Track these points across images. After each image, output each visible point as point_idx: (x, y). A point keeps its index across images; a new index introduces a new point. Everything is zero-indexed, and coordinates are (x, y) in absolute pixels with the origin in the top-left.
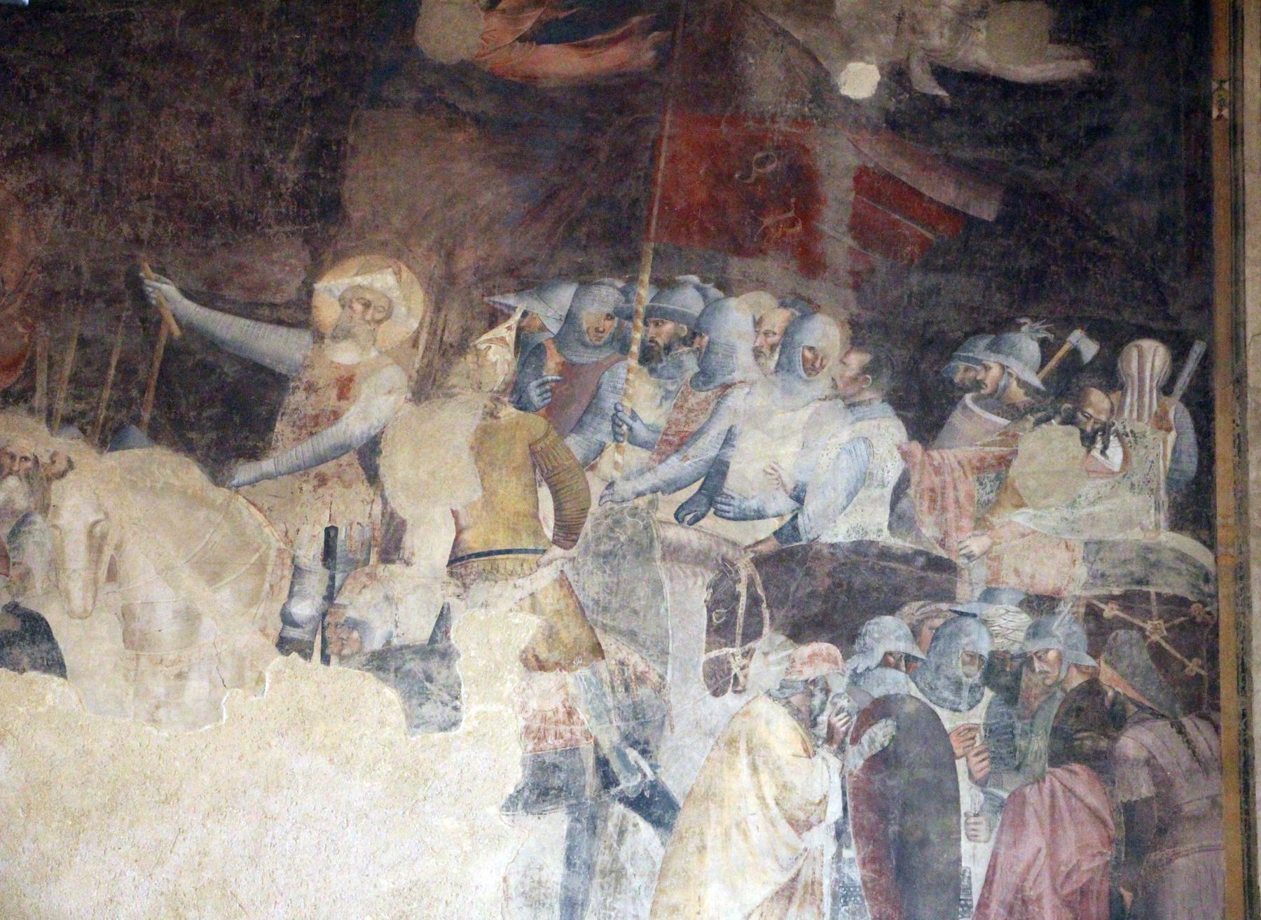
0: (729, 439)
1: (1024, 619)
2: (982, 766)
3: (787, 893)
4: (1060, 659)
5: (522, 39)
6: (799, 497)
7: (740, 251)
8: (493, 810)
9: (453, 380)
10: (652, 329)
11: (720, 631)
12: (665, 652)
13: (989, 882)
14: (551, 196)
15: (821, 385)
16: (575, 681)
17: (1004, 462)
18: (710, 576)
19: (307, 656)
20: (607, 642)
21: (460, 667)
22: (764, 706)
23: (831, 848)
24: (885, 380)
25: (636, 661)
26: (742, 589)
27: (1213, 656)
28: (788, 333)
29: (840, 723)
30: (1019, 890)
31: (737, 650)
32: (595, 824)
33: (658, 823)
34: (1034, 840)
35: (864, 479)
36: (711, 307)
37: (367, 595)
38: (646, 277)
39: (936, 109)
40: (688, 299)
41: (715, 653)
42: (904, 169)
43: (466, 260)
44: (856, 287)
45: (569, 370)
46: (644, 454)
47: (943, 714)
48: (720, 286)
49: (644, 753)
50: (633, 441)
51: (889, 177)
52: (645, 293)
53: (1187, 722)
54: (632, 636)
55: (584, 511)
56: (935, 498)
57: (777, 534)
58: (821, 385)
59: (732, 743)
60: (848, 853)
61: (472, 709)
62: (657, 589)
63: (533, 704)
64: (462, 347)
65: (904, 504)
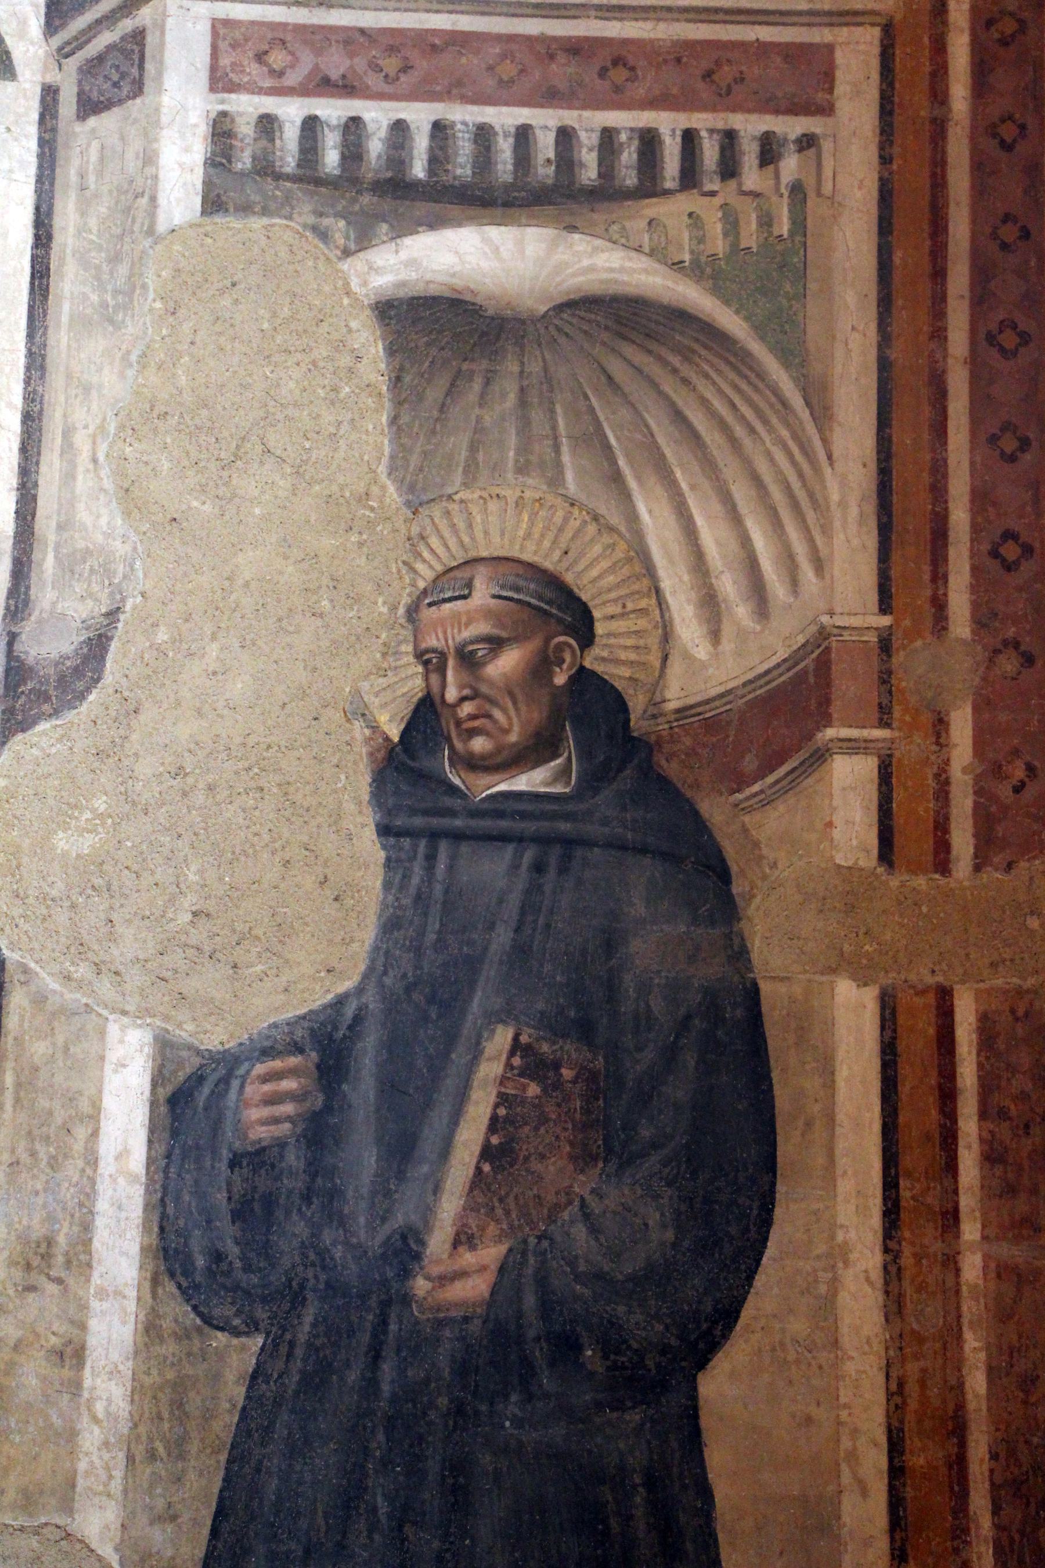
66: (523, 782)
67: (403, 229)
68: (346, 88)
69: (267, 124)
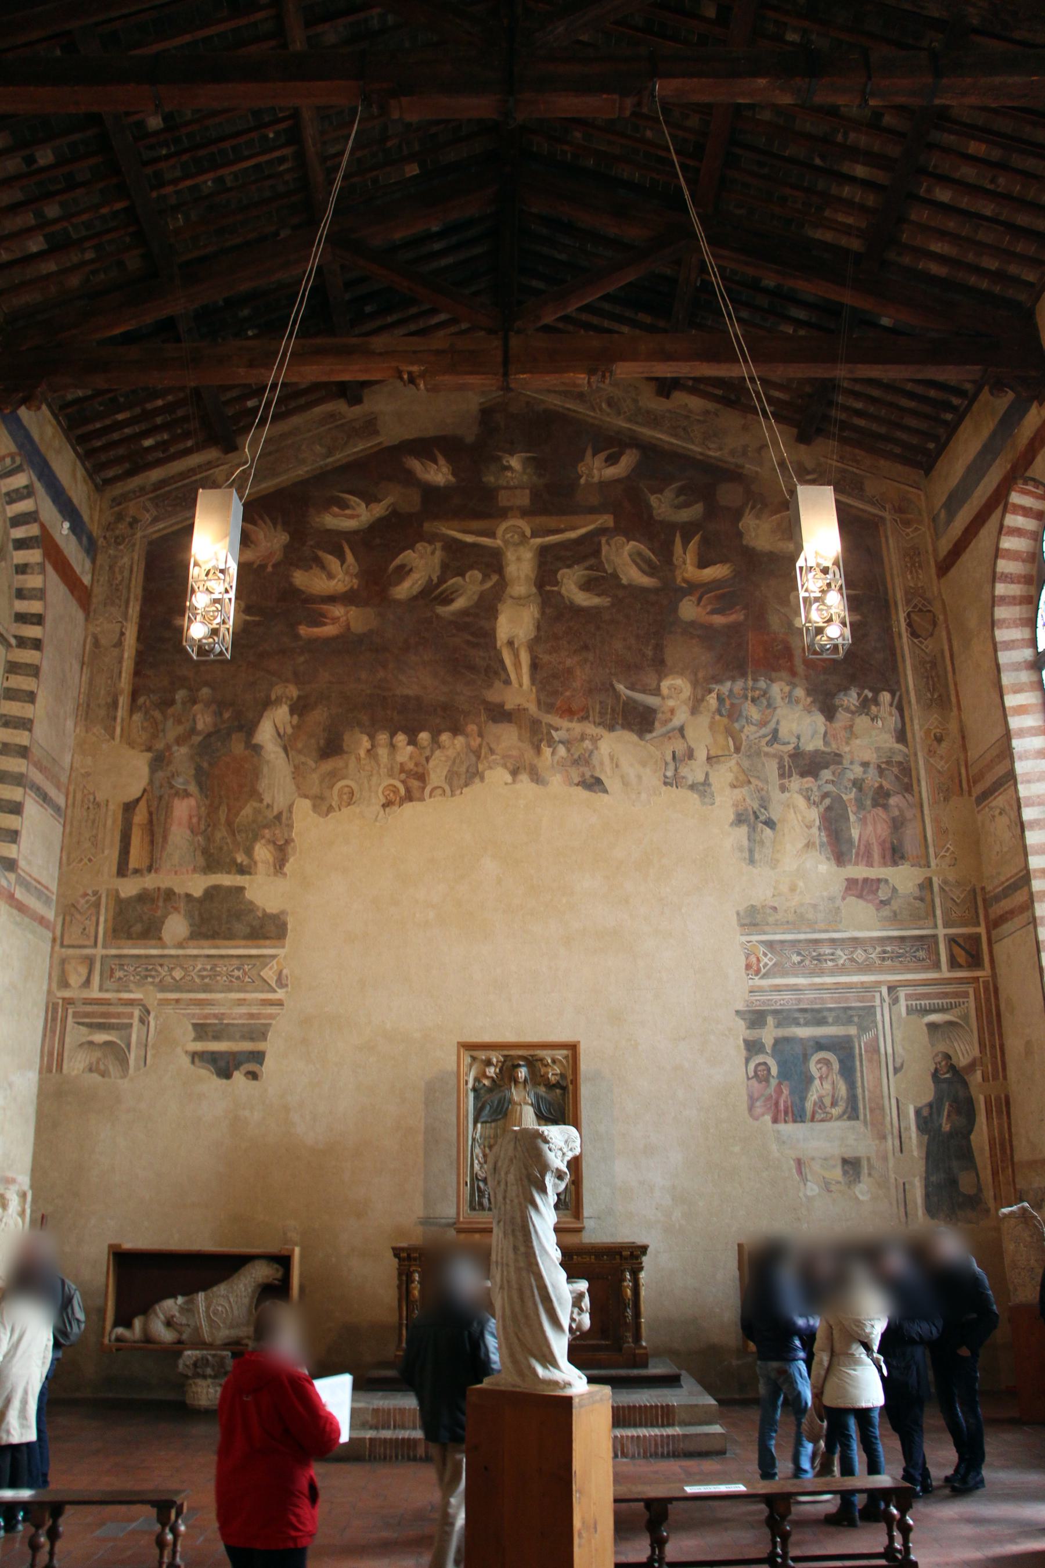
0: (778, 723)
1: (861, 769)
2: (854, 809)
4: (872, 779)
5: (708, 613)
6: (798, 737)
7: (774, 670)
8: (727, 827)
9: (701, 709)
10: (753, 693)
11: (782, 776)
12: (767, 782)
15: (801, 707)
16: (744, 790)
17: (851, 726)
18: (777, 761)
19: (672, 786)
20: (752, 780)
21: (713, 788)
22: (796, 795)
23: (817, 833)
25: (760, 784)
26: (786, 764)
28: (790, 692)
29: (816, 799)
30: (868, 841)
31: (787, 780)
34: (870, 828)
35: (815, 733)
36: (768, 686)
37: (686, 770)
38: (750, 678)
40: (762, 684)
41: (781, 782)
43: (701, 675)
44: (807, 679)
45: (732, 705)
47: (843, 796)
48: (770, 680)
49: (765, 809)
50: (752, 724)
52: (750, 683)
53: (906, 795)
54: (758, 778)
55: (741, 744)
56: (834, 737)
57: (794, 748)
58: (801, 707)
59: (788, 806)
60: (823, 834)
61: (718, 799)
62: (764, 765)
63: (734, 797)
64: (702, 700)
65: (827, 739)
66: (947, 1076)
67: (927, 1015)
68: (919, 999)
69: (912, 1005)
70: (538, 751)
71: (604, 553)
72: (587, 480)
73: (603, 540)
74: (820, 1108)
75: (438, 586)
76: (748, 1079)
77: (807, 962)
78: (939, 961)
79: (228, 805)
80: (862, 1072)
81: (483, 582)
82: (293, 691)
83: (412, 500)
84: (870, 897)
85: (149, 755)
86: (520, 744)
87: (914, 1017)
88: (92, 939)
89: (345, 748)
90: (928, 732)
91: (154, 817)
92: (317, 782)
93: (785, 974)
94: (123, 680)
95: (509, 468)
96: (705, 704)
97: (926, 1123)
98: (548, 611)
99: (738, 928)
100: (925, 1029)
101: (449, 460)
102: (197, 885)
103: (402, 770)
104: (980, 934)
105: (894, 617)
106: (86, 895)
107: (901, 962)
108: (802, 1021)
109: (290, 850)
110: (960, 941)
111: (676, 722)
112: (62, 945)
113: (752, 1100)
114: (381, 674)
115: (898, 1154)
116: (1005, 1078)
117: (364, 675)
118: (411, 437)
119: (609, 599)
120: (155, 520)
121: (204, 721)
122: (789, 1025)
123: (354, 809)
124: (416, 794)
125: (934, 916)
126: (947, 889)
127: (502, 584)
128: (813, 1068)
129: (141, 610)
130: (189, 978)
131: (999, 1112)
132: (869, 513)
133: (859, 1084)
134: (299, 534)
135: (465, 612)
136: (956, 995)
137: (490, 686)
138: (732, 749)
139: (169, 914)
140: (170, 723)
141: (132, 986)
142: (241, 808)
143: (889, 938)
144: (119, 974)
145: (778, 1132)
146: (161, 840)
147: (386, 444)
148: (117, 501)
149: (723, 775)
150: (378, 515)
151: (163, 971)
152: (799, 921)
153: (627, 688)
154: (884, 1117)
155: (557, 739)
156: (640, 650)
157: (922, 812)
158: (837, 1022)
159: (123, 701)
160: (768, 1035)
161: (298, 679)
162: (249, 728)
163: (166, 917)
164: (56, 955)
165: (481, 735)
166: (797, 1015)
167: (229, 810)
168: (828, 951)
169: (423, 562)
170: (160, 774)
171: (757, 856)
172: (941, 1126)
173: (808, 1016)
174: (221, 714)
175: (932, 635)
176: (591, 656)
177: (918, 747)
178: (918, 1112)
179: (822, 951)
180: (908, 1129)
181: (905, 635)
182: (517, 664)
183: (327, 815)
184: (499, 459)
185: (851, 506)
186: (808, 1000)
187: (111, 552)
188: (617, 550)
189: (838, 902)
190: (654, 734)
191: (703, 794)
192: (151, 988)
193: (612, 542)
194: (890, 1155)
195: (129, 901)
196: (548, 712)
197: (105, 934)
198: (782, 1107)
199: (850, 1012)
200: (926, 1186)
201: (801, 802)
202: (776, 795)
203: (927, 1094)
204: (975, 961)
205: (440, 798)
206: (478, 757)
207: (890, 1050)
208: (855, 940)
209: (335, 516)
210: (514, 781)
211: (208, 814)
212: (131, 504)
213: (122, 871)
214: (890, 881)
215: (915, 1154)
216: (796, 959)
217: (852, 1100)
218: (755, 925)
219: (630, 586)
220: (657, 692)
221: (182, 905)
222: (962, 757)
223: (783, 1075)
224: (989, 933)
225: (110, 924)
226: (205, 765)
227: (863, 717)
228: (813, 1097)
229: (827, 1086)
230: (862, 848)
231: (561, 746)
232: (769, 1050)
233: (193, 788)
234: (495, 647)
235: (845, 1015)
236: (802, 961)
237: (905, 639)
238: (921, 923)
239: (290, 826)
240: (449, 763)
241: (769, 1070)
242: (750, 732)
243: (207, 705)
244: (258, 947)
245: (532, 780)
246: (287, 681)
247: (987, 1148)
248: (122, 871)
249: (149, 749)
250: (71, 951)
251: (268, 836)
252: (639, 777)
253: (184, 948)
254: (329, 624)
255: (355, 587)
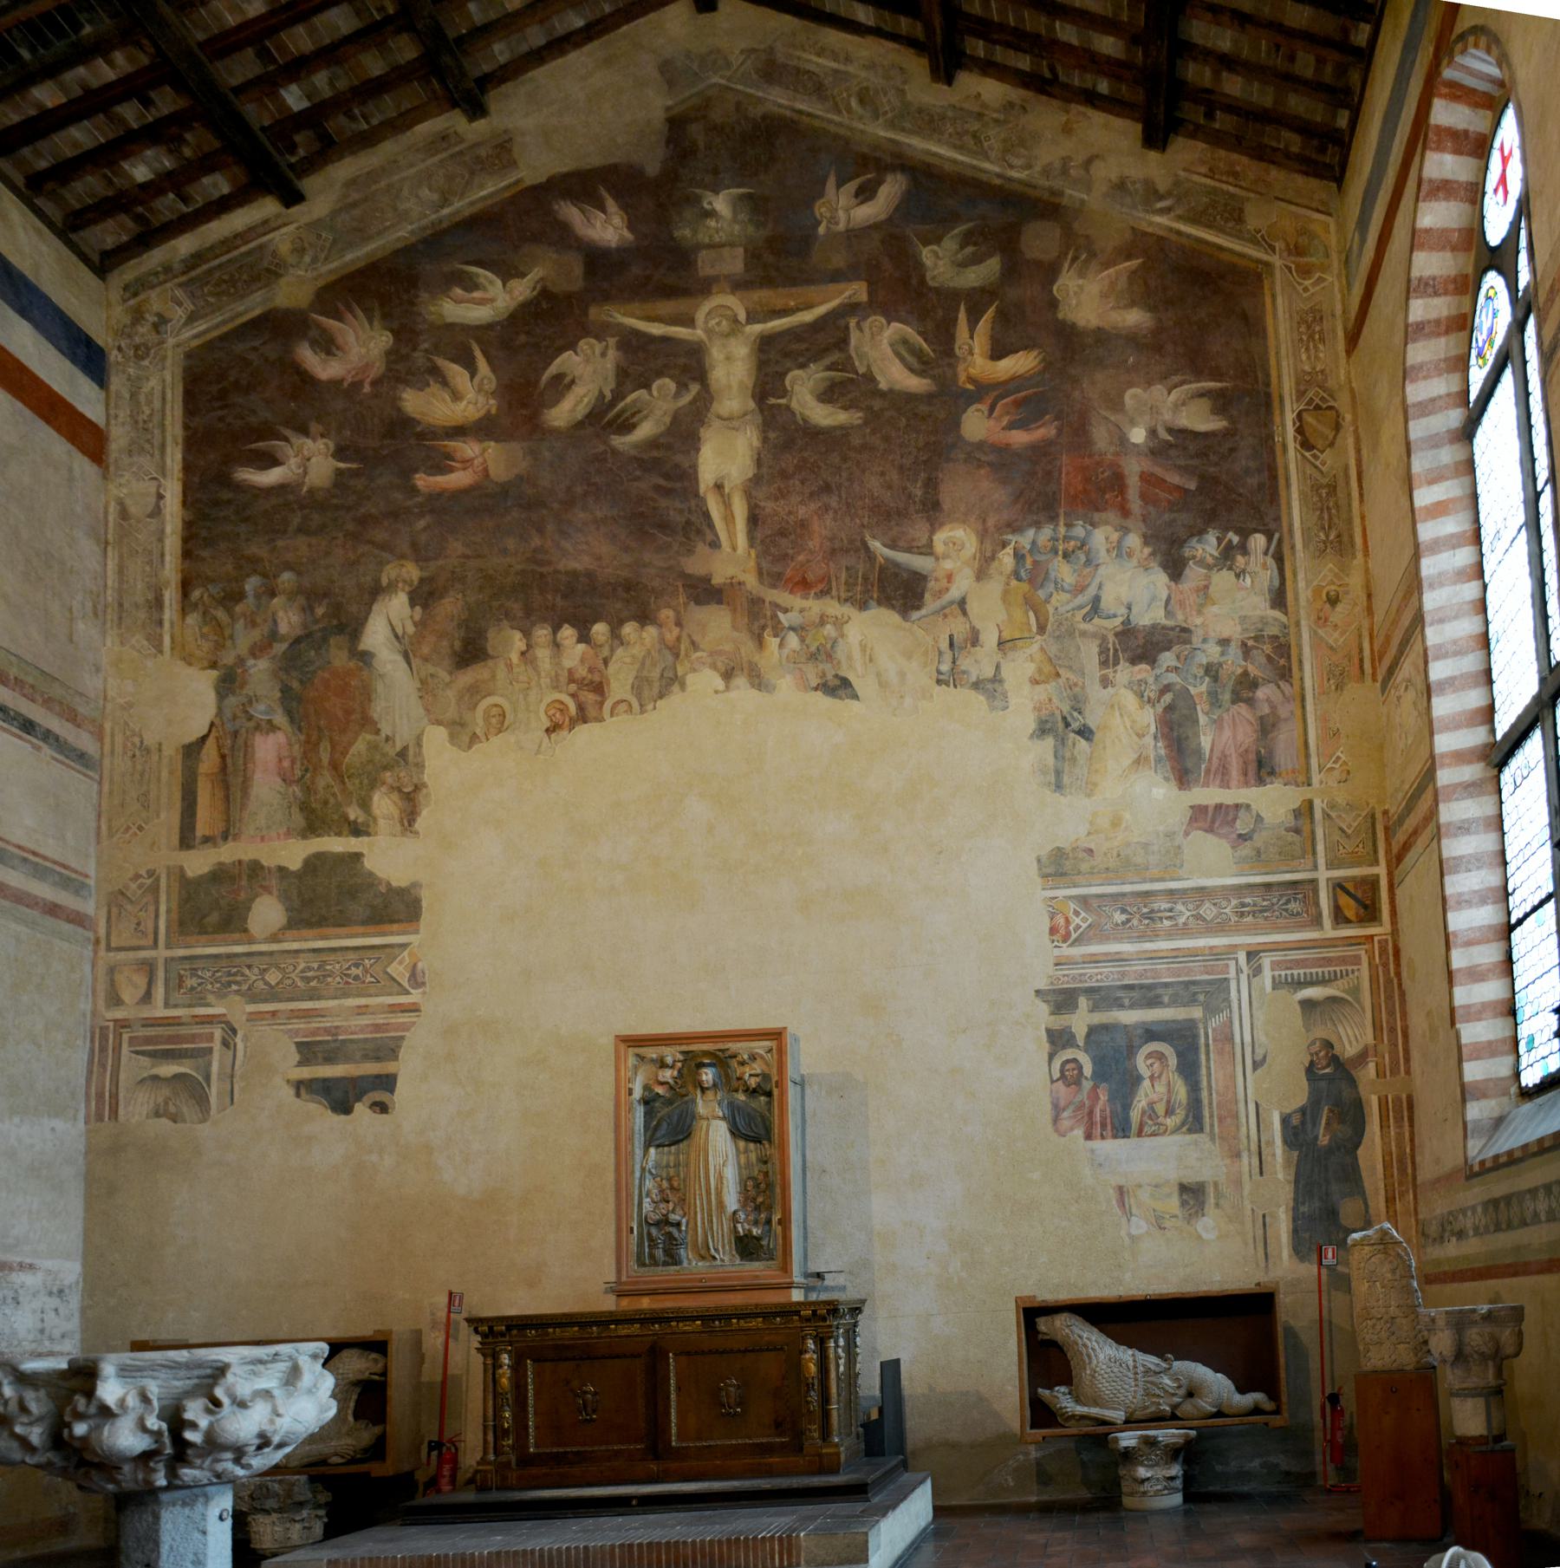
0: (1100, 587)
1: (1218, 649)
2: (1207, 707)
3: (1138, 761)
7: (1097, 510)
11: (1104, 664)
13: (1212, 750)
14: (1021, 493)
15: (1134, 562)
16: (1051, 687)
17: (1206, 587)
18: (1098, 642)
20: (1061, 671)
21: (1007, 686)
22: (1123, 691)
23: (1153, 743)
24: (1158, 558)
27: (1289, 657)
28: (1119, 542)
29: (1152, 695)
32: (1063, 741)
33: (1087, 739)
34: (1227, 733)
35: (1153, 599)
36: (1088, 533)
39: (1171, 446)
40: (1079, 531)
42: (1159, 471)
43: (991, 522)
45: (1035, 563)
46: (1068, 596)
51: (1152, 474)
52: (1062, 530)
54: (1070, 668)
58: (1134, 562)
60: (1160, 744)
61: (1013, 701)
62: (1079, 649)
64: (993, 558)
70: (760, 642)
71: (853, 342)
72: (828, 228)
73: (853, 323)
74: (1150, 1118)
75: (612, 404)
76: (1053, 1082)
77: (1135, 922)
78: (1320, 915)
79: (331, 740)
80: (1208, 1068)
81: (677, 395)
82: (412, 572)
83: (564, 272)
84: (1225, 830)
85: (214, 674)
86: (736, 634)
87: (1282, 992)
88: (151, 937)
89: (490, 651)
90: (1317, 591)
91: (229, 761)
92: (453, 701)
93: (1104, 938)
94: (167, 566)
95: (711, 214)
96: (995, 564)
97: (1296, 1135)
98: (772, 435)
99: (1039, 880)
100: (1298, 1008)
101: (624, 207)
102: (293, 853)
103: (571, 680)
104: (1378, 876)
105: (1277, 419)
106: (137, 876)
107: (1266, 918)
108: (1126, 1002)
109: (421, 797)
110: (1350, 886)
111: (955, 593)
112: (109, 948)
113: (1057, 1110)
114: (536, 541)
115: (1256, 1177)
116: (1408, 1072)
117: (511, 543)
118: (565, 170)
119: (860, 414)
120: (192, 318)
121: (289, 620)
122: (1109, 1008)
123: (508, 738)
124: (591, 712)
125: (1314, 853)
126: (1333, 814)
127: (706, 397)
128: (1142, 1064)
129: (184, 459)
130: (289, 982)
131: (1399, 1119)
132: (1250, 258)
133: (1204, 1084)
134: (405, 334)
135: (653, 443)
136: (1343, 960)
137: (690, 552)
138: (1034, 629)
139: (257, 896)
140: (240, 625)
141: (211, 998)
142: (351, 744)
143: (1250, 886)
144: (191, 982)
145: (1092, 1151)
146: (239, 794)
147: (528, 182)
148: (134, 289)
149: (1019, 669)
150: (521, 298)
151: (252, 975)
152: (1124, 866)
153: (885, 545)
154: (1238, 1127)
155: (786, 625)
156: (905, 489)
157: (1304, 707)
158: (1175, 1002)
159: (171, 596)
160: (1080, 1021)
161: (419, 554)
162: (350, 627)
163: (252, 900)
164: (100, 962)
165: (679, 624)
166: (1120, 994)
167: (333, 747)
168: (1165, 906)
169: (590, 369)
170: (232, 701)
171: (1066, 780)
172: (1316, 1138)
173: (1135, 994)
174: (312, 609)
175: (1332, 444)
176: (833, 502)
177: (1302, 612)
178: (1285, 1120)
179: (1156, 906)
180: (1271, 1143)
181: (1292, 445)
182: (729, 518)
183: (470, 747)
184: (698, 200)
185: (1220, 248)
186: (1134, 973)
187: (131, 371)
188: (873, 337)
189: (1179, 839)
190: (923, 612)
191: (991, 696)
192: (237, 998)
193: (866, 325)
194: (1246, 1177)
195: (199, 881)
196: (774, 586)
197: (168, 928)
198: (1098, 1118)
199: (1194, 989)
200: (1294, 1220)
201: (1129, 700)
202: (1096, 693)
203: (1300, 1096)
204: (1369, 912)
205: (625, 716)
206: (677, 656)
207: (1248, 1038)
208: (1202, 889)
209: (458, 301)
210: (727, 688)
211: (305, 755)
212: (153, 294)
213: (187, 839)
214: (1253, 807)
215: (1280, 1176)
216: (1119, 917)
217: (1195, 1106)
218: (1063, 874)
219: (891, 391)
220: (928, 550)
221: (274, 882)
222: (1366, 624)
223: (1100, 1075)
224: (1390, 874)
225: (175, 916)
226: (295, 685)
227: (1225, 572)
228: (1140, 1103)
229: (1161, 1088)
230: (1215, 761)
231: (792, 634)
232: (1081, 1044)
233: (280, 718)
234: (697, 495)
235: (1187, 992)
236: (1128, 921)
237: (1291, 453)
238: (1296, 862)
239: (420, 766)
240: (637, 666)
241: (1080, 1068)
242: (1060, 603)
243: (292, 596)
244: (384, 934)
245: (753, 686)
246: (403, 557)
247: (1380, 1167)
248: (187, 839)
249: (213, 665)
250: (122, 956)
251: (389, 780)
252: (902, 675)
253: (280, 941)
254: (458, 469)
255: (493, 411)
